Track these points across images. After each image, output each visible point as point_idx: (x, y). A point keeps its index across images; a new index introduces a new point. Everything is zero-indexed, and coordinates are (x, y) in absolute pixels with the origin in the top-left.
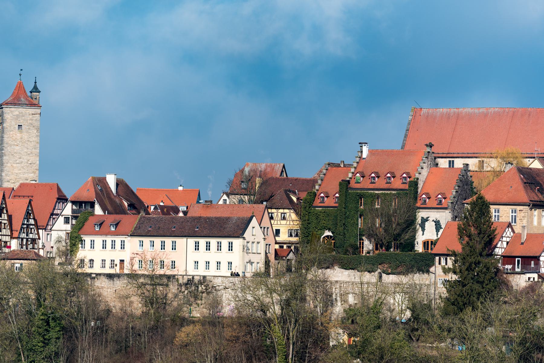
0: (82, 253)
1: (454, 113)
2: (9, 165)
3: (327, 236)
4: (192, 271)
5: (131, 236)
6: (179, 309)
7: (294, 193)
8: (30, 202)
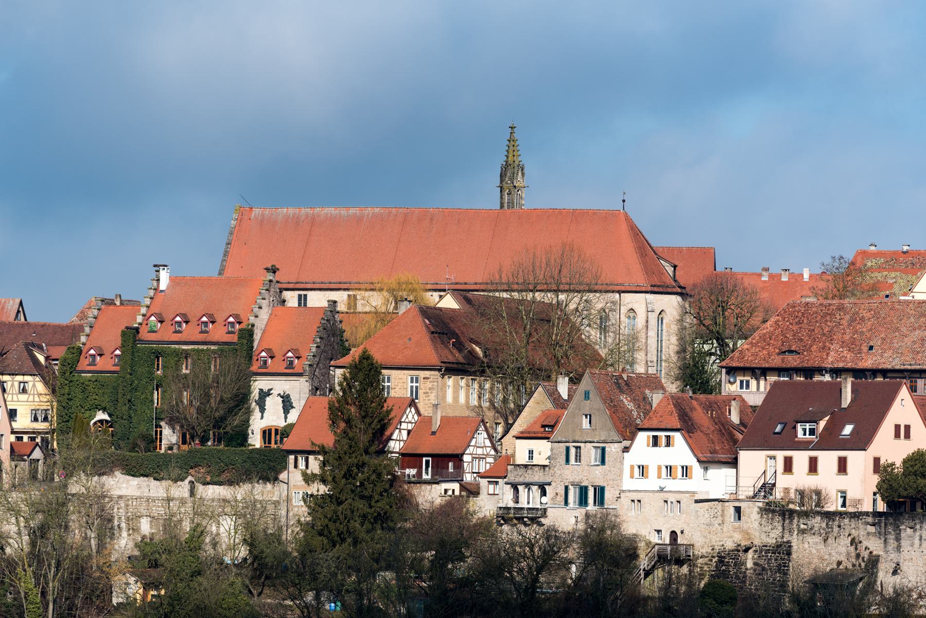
1: (307, 215)
3: (101, 421)
7: (40, 348)
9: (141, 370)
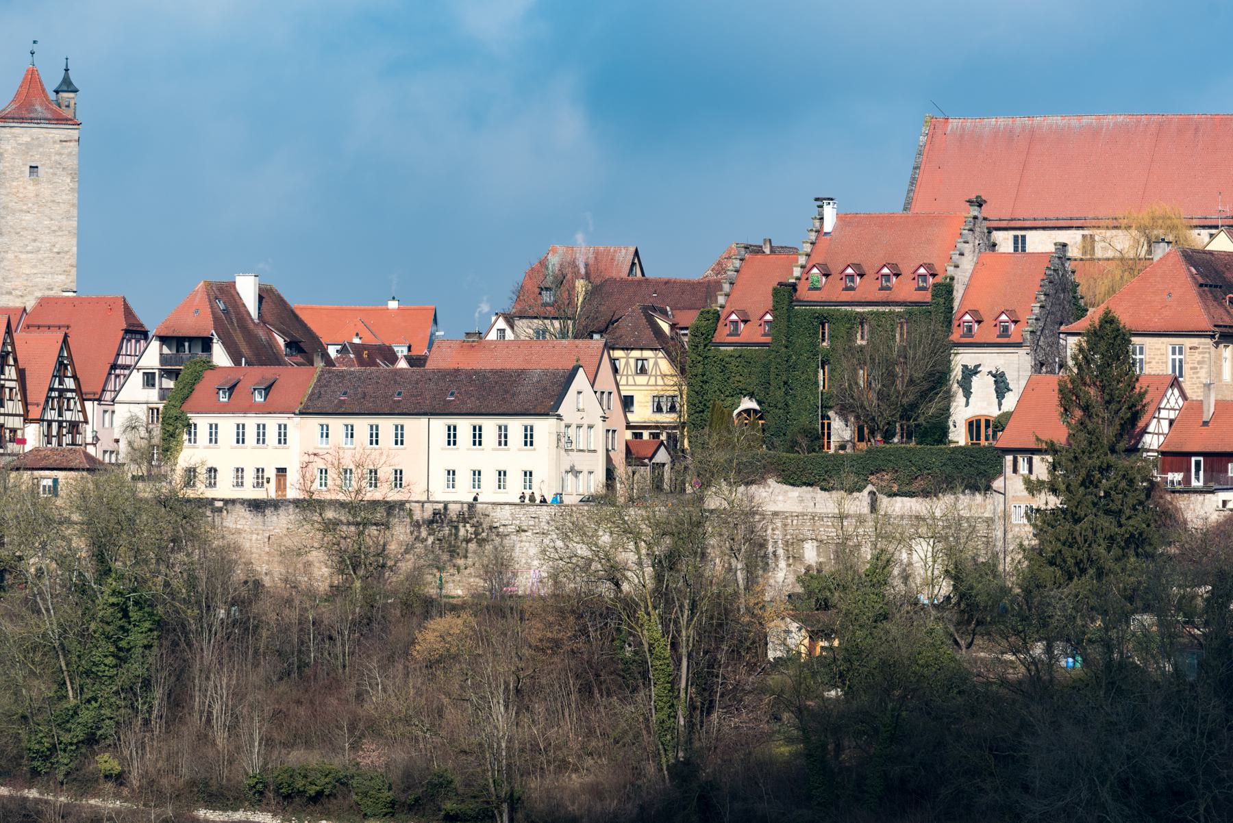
0: (188, 455)
1: (1024, 127)
2: (10, 256)
3: (747, 411)
4: (440, 493)
5: (301, 413)
6: (415, 577)
7: (664, 313)
8: (65, 341)
9: (801, 341)
